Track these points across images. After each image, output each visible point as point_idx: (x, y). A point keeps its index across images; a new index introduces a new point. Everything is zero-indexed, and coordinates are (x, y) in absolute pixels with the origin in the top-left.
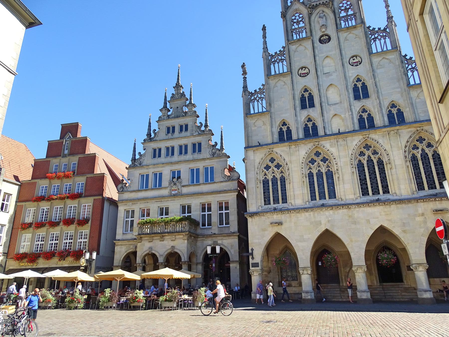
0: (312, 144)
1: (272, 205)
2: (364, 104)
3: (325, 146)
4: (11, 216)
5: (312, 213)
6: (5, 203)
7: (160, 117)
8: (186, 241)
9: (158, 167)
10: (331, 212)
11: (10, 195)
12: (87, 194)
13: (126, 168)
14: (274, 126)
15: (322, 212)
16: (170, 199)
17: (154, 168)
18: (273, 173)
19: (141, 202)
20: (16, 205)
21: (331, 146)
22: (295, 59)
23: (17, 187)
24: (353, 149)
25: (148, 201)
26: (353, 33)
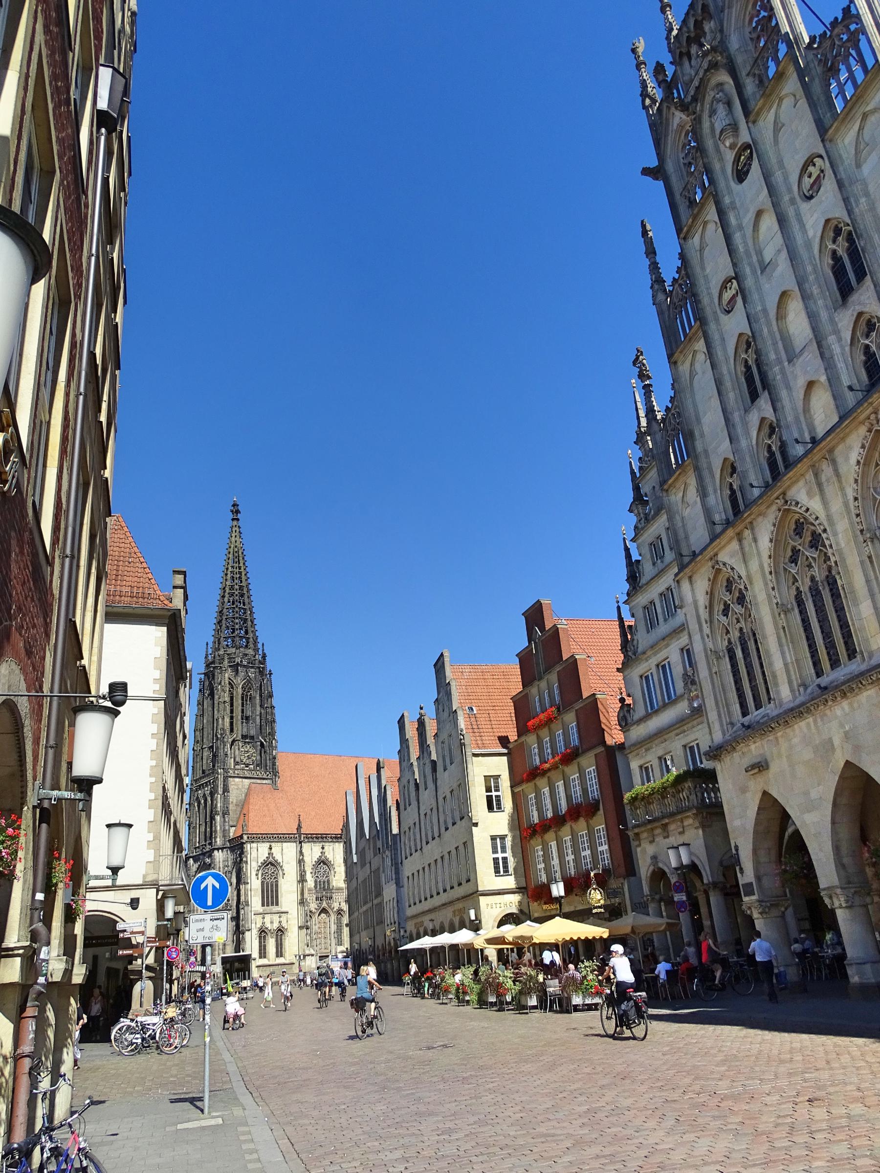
0: (774, 507)
1: (755, 715)
2: (859, 308)
3: (799, 500)
4: (512, 817)
5: (811, 720)
6: (494, 794)
7: (636, 527)
8: (700, 832)
9: (660, 650)
10: (845, 704)
11: (497, 777)
12: (584, 747)
13: (618, 670)
14: (710, 489)
15: (828, 712)
16: (695, 722)
17: (655, 654)
18: (738, 621)
19: (656, 742)
20: (514, 794)
21: (810, 494)
22: (708, 271)
23: (505, 758)
24: (856, 481)
25: (665, 737)
26: (786, 95)
